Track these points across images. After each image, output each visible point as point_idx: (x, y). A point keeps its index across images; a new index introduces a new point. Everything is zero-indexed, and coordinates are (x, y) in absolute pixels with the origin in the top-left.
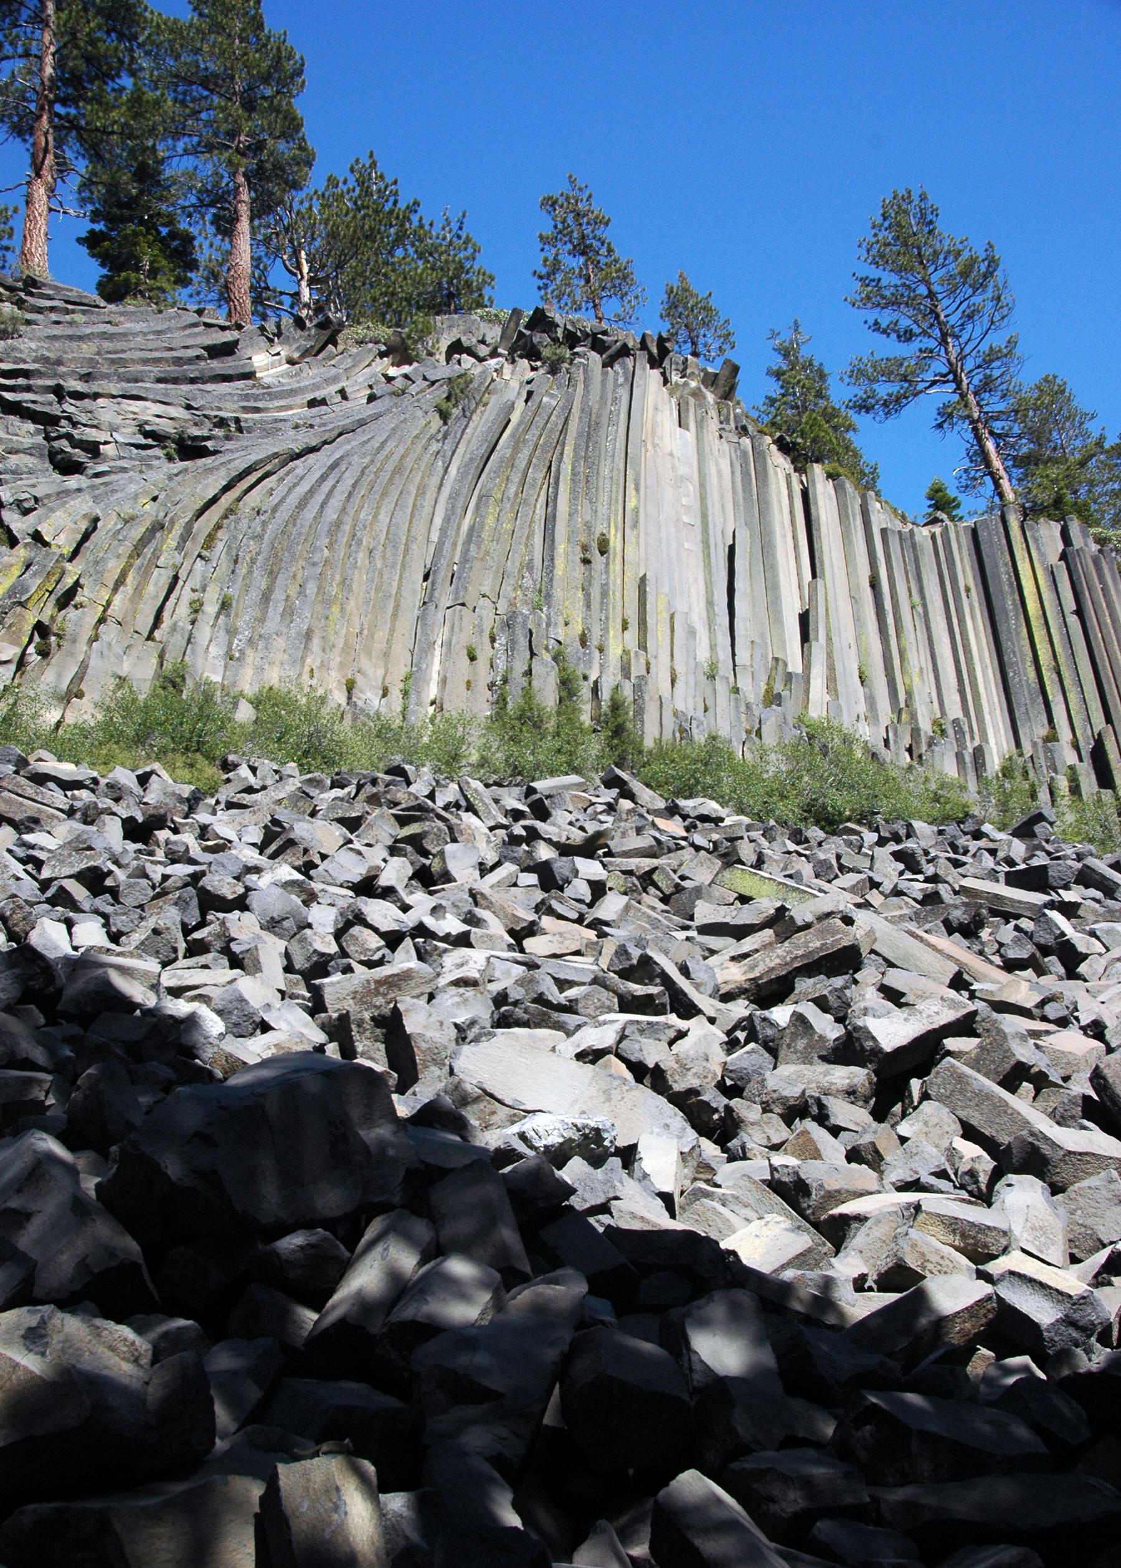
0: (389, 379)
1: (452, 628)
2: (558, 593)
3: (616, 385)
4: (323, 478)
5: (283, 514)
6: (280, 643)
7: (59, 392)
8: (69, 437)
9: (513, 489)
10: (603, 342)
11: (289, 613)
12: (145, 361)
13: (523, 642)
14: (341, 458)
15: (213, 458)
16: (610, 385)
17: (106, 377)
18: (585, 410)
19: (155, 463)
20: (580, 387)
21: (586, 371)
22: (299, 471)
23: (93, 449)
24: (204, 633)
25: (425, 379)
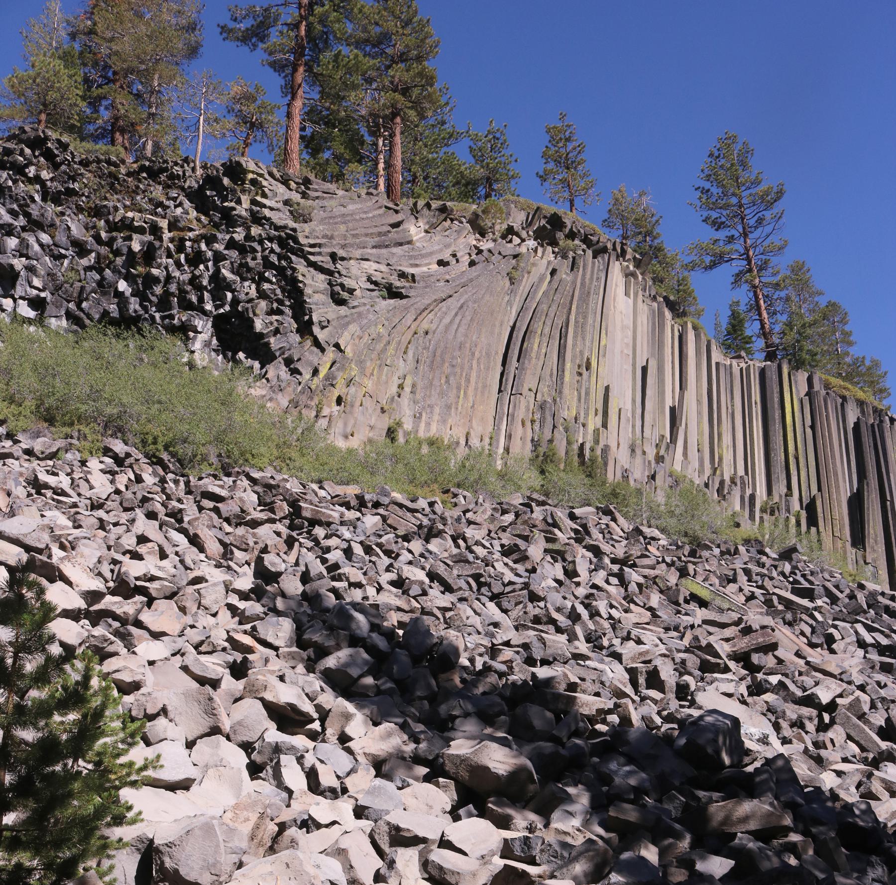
0: (480, 252)
1: (515, 406)
2: (566, 391)
3: (599, 270)
4: (456, 314)
5: (437, 336)
6: (437, 410)
7: (334, 257)
8: (342, 286)
9: (547, 330)
10: (591, 240)
11: (442, 394)
12: (366, 235)
13: (549, 419)
14: (464, 303)
15: (406, 300)
16: (596, 268)
17: (352, 245)
18: (583, 284)
19: (377, 300)
20: (581, 269)
21: (584, 261)
22: (444, 309)
23: (351, 291)
24: (405, 401)
25: (500, 253)
